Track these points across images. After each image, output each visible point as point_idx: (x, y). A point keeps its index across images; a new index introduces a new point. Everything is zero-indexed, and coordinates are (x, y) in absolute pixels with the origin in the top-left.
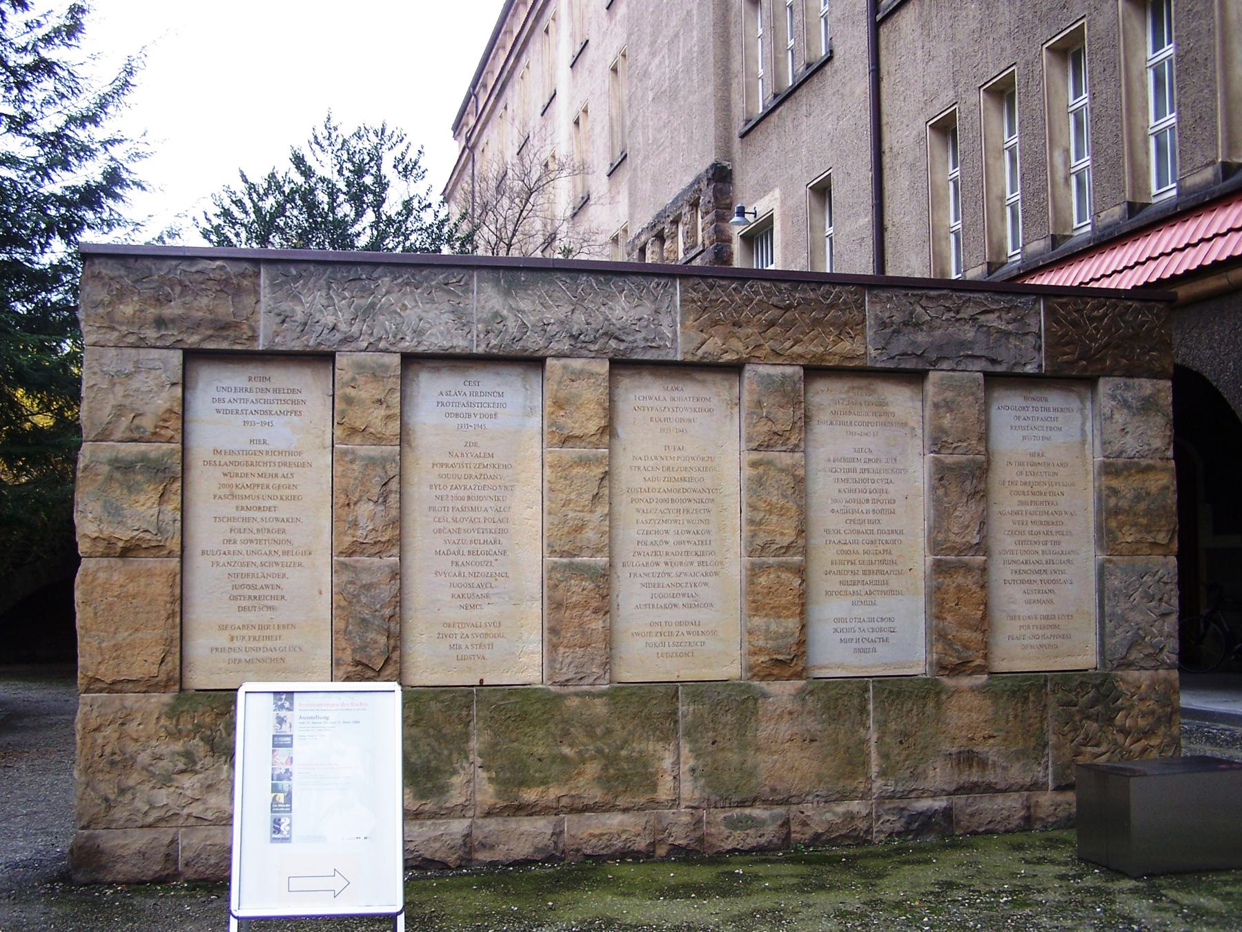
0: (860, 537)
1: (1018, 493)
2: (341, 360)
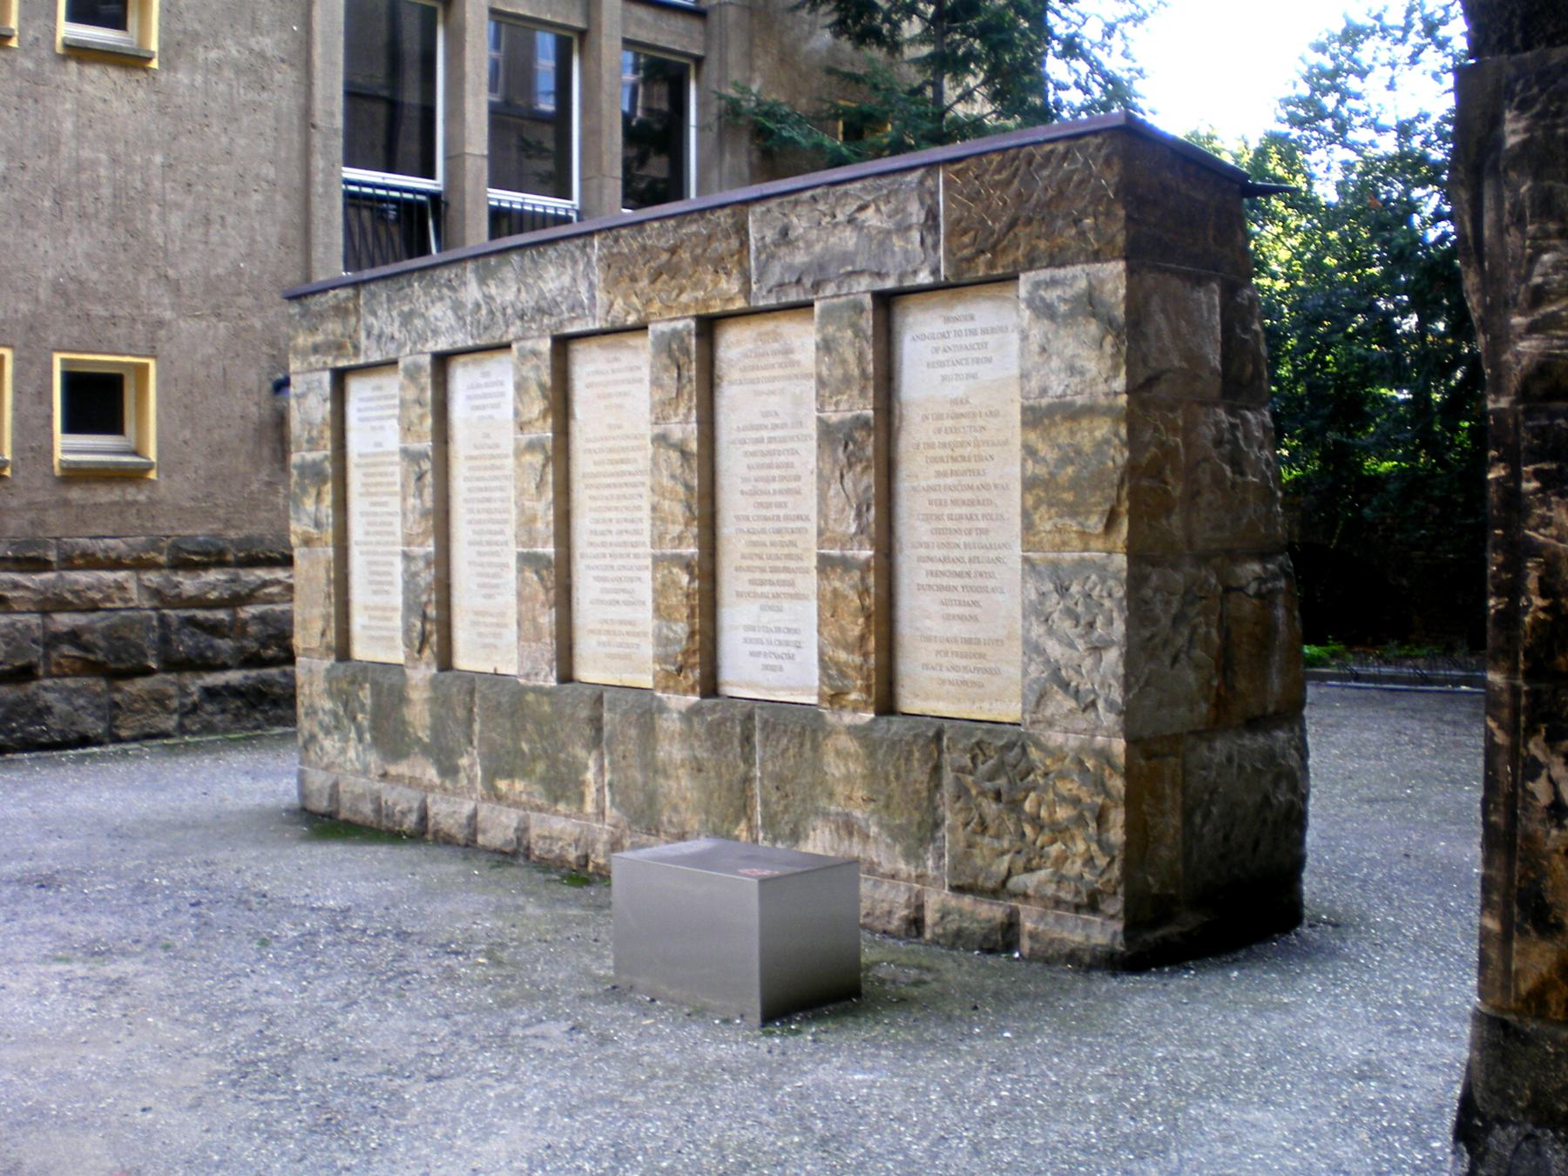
0: (769, 525)
1: (935, 460)
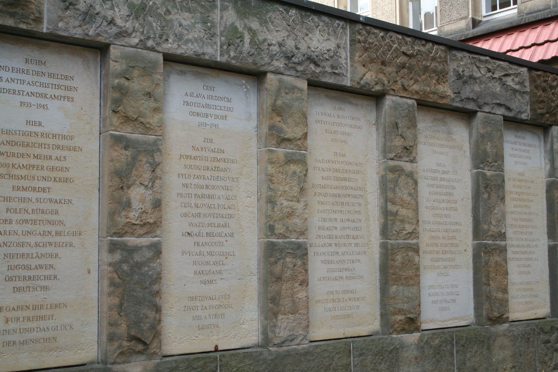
2: (114, 51)
